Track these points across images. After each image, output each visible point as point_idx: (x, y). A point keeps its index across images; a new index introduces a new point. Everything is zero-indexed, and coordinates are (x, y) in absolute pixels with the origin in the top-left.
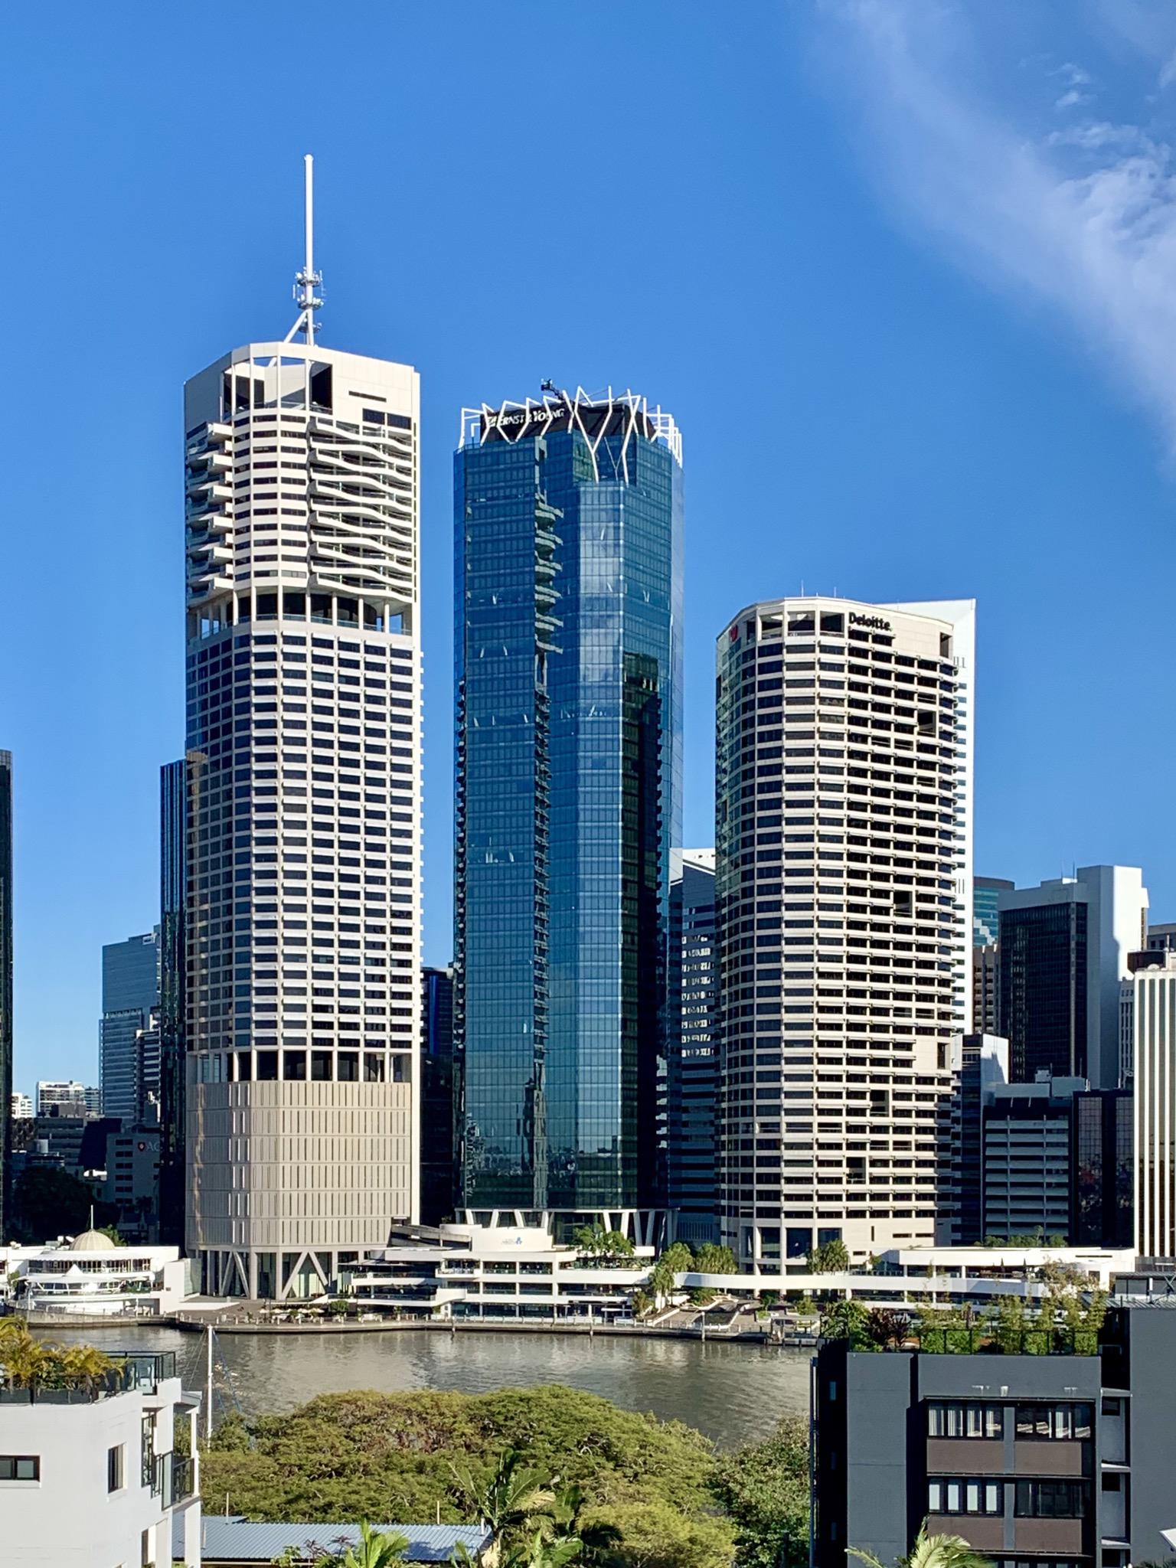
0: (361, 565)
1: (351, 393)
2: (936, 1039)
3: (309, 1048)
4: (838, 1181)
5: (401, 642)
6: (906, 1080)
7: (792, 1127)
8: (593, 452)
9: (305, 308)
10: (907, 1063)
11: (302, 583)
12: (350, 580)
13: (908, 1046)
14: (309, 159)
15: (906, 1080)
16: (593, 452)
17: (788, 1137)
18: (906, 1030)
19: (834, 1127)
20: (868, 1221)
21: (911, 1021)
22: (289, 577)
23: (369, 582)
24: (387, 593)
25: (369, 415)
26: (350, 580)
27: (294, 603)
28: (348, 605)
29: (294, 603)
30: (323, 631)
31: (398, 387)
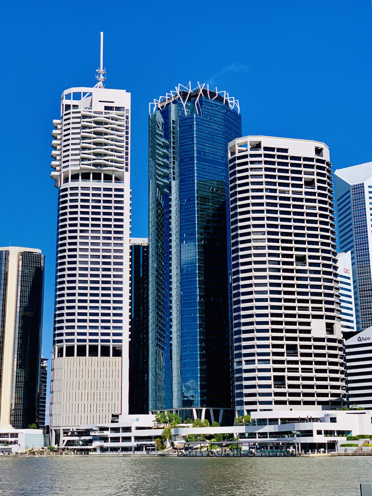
1: (100, 101)
2: (325, 321)
4: (269, 386)
5: (118, 186)
6: (309, 339)
7: (247, 362)
8: (184, 105)
9: (99, 81)
10: (309, 332)
13: (308, 324)
14: (102, 33)
15: (309, 339)
16: (184, 105)
17: (245, 367)
18: (307, 316)
21: (310, 312)
22: (74, 167)
23: (106, 166)
25: (106, 108)
27: (75, 177)
31: (122, 98)
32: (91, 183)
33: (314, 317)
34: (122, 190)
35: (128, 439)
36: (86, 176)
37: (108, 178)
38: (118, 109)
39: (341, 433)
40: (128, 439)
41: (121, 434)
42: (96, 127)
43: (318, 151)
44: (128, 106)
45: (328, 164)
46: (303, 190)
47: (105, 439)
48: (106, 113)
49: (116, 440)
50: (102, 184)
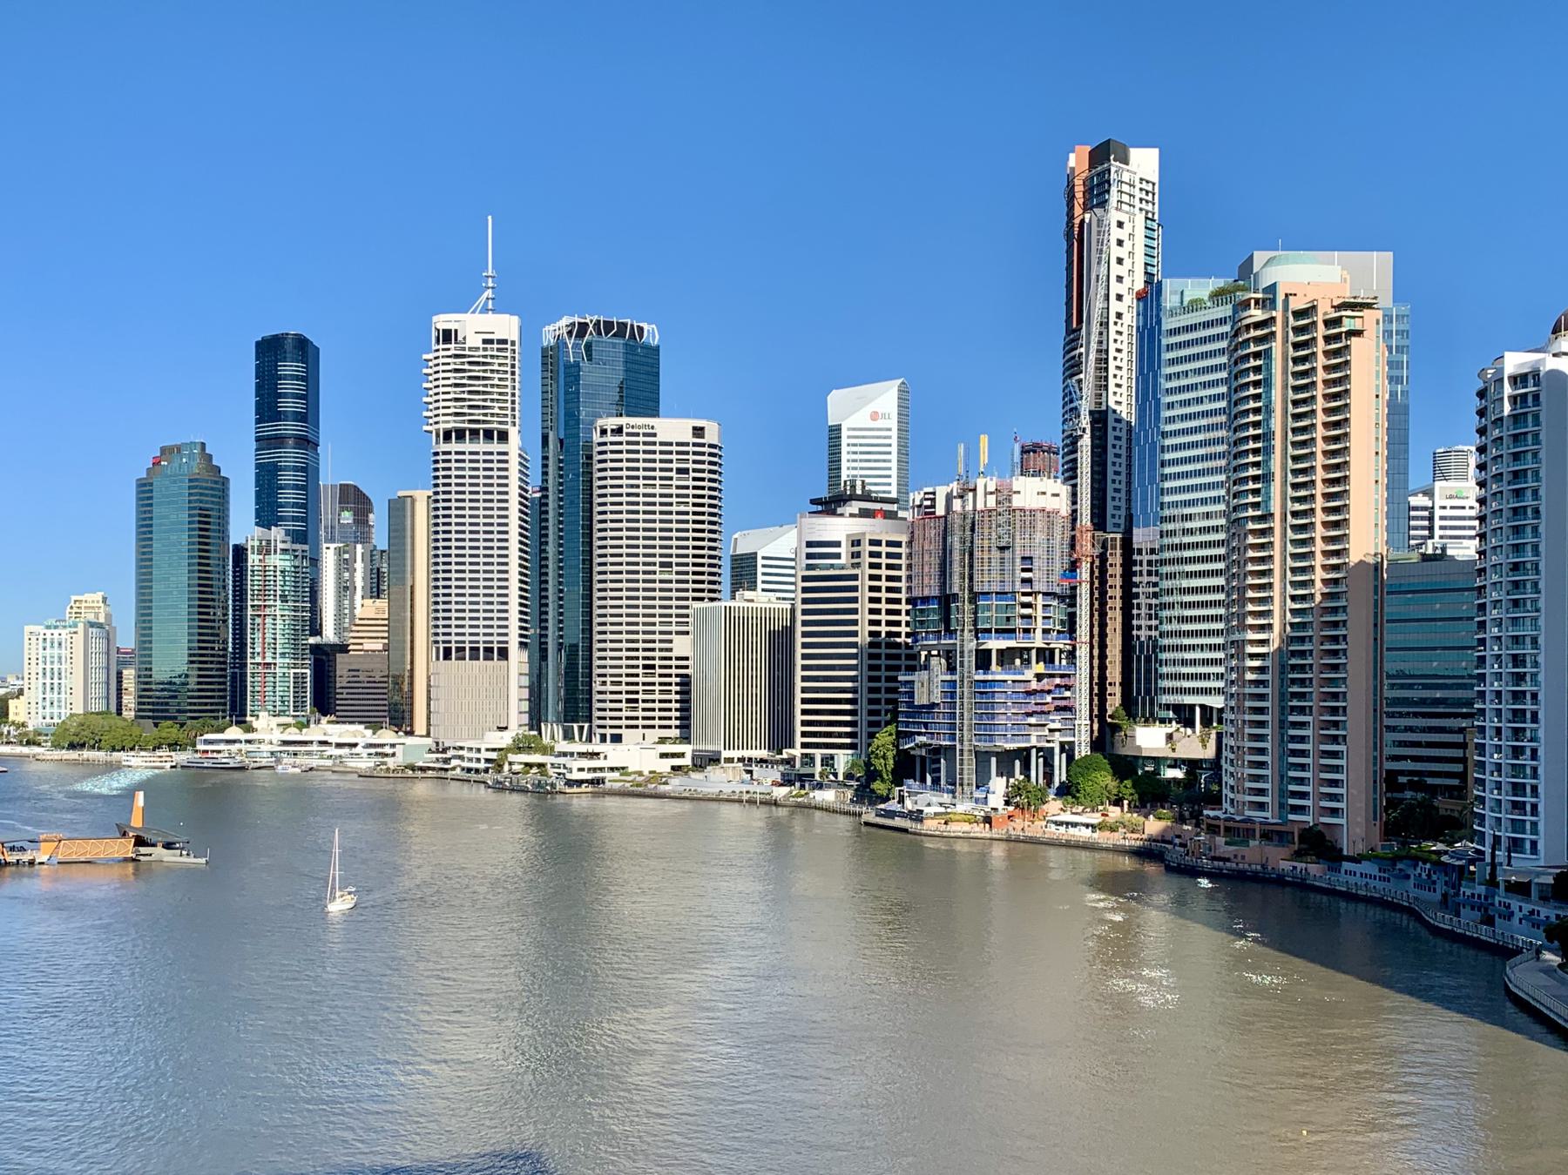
0: (478, 414)
3: (453, 646)
10: (670, 650)
11: (449, 426)
12: (470, 421)
13: (671, 641)
19: (620, 683)
20: (641, 731)
21: (674, 628)
23: (484, 422)
24: (495, 426)
25: (485, 341)
26: (470, 421)
27: (447, 436)
28: (475, 433)
29: (447, 436)
31: (507, 326)
32: (467, 446)
33: (678, 633)
34: (506, 454)
35: (478, 760)
36: (460, 435)
37: (489, 435)
39: (612, 769)
40: (478, 760)
41: (474, 755)
42: (473, 369)
43: (698, 431)
44: (515, 336)
45: (711, 446)
46: (674, 483)
47: (461, 758)
48: (485, 349)
49: (470, 760)
50: (482, 446)
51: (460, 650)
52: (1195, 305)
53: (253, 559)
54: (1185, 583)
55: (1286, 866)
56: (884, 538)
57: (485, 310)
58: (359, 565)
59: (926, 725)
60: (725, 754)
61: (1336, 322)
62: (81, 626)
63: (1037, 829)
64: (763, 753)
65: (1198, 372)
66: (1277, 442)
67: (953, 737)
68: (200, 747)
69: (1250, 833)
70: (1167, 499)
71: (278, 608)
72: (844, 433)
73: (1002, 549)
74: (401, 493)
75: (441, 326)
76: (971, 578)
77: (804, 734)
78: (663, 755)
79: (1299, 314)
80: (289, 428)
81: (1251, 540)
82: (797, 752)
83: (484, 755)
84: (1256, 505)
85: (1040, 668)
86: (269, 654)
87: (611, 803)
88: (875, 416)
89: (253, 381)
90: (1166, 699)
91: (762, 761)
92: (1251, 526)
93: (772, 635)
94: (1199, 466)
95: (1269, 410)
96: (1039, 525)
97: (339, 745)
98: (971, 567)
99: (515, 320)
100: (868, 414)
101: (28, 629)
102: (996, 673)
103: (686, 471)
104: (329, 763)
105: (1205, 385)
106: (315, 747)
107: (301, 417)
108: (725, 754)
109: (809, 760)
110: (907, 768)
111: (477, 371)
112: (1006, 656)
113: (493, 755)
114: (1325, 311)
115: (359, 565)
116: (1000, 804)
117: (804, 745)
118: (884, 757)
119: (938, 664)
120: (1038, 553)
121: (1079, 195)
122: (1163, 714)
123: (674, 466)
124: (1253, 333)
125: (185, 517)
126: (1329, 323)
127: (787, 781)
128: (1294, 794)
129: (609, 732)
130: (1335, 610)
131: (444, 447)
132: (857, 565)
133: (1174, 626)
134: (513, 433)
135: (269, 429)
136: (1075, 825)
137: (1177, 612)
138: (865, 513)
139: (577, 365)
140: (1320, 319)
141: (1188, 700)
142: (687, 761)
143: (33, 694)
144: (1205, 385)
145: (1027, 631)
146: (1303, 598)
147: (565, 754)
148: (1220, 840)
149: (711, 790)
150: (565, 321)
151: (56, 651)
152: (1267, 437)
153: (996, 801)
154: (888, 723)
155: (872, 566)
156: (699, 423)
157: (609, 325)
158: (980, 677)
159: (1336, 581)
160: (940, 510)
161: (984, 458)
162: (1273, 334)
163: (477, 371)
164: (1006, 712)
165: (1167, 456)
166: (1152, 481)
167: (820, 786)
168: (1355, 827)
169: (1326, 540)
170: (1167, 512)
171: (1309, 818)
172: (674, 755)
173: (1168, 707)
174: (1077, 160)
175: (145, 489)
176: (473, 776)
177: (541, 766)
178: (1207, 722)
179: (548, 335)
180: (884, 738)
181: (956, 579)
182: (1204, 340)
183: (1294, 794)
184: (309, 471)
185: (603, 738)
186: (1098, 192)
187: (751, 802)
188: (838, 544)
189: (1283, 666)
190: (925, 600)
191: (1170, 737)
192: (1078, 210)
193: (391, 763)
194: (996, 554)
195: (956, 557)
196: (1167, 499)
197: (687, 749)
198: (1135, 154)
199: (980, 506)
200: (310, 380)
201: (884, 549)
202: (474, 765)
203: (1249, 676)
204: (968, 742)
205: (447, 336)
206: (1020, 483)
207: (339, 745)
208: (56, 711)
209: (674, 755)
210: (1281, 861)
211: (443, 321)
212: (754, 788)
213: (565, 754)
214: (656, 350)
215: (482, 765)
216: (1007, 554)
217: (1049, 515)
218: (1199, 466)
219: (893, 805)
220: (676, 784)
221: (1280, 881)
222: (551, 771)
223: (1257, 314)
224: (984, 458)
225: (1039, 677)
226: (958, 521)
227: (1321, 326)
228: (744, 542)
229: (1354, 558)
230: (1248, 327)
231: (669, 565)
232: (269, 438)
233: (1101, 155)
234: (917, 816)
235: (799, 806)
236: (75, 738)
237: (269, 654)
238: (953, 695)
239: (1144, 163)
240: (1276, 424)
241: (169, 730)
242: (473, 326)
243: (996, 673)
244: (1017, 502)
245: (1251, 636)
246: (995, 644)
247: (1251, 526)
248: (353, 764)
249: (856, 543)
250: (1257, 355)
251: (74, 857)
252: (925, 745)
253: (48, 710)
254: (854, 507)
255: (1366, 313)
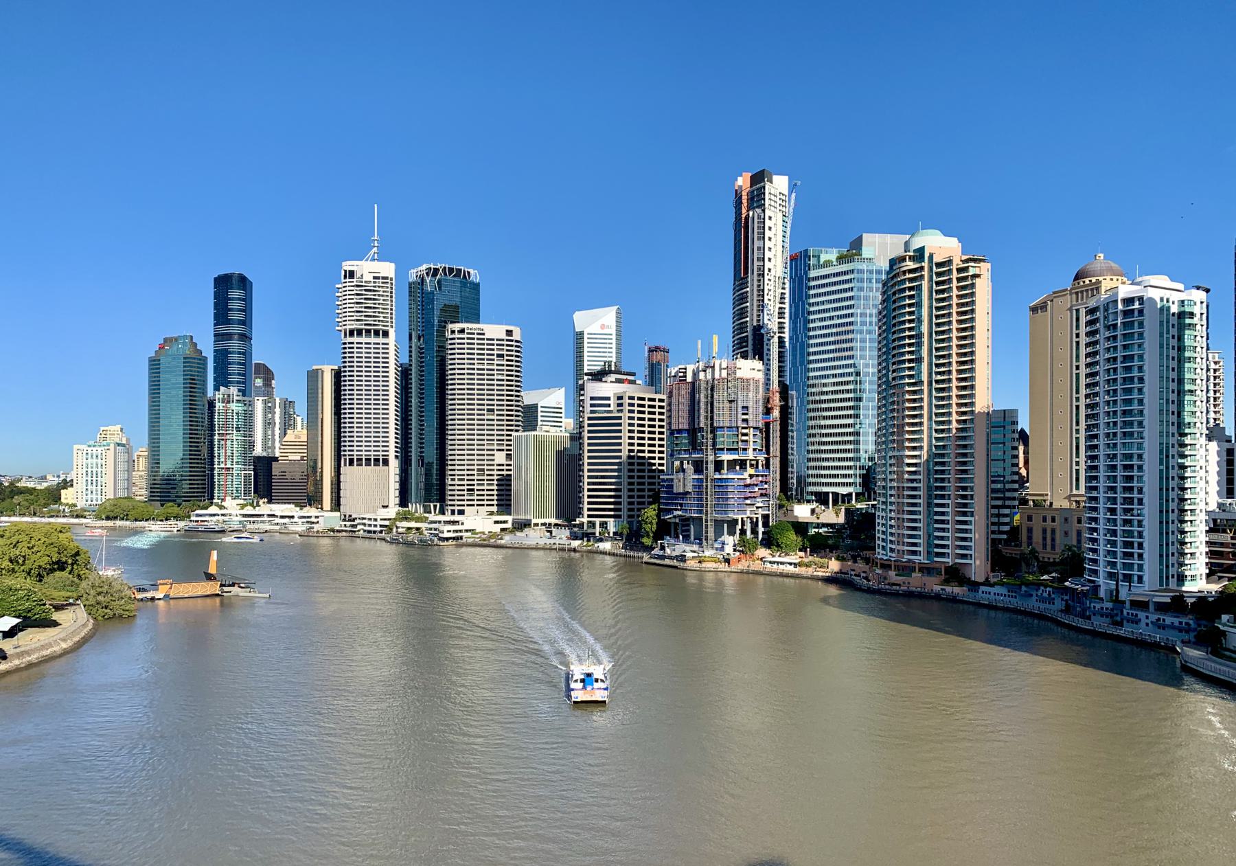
5: (385, 340)
21: (496, 447)
27: (352, 333)
28: (368, 331)
29: (352, 333)
30: (368, 340)
31: (387, 269)
32: (364, 339)
36: (360, 332)
37: (377, 333)
38: (384, 278)
41: (373, 523)
42: (368, 293)
43: (509, 333)
44: (392, 274)
50: (373, 339)
51: (377, 460)
52: (828, 264)
53: (219, 406)
54: (823, 422)
55: (937, 588)
56: (636, 395)
57: (373, 260)
58: (277, 410)
59: (681, 505)
60: (534, 521)
61: (965, 269)
62: (112, 446)
63: (757, 566)
64: (553, 521)
65: (830, 302)
66: (925, 339)
67: (700, 512)
68: (193, 518)
69: (913, 570)
70: (811, 374)
71: (235, 435)
72: (586, 336)
73: (730, 402)
74: (315, 367)
75: (348, 268)
76: (712, 418)
77: (589, 510)
78: (496, 522)
79: (939, 265)
80: (235, 329)
81: (907, 397)
82: (585, 520)
83: (379, 522)
84: (911, 377)
85: (752, 471)
86: (229, 463)
87: (464, 549)
88: (603, 327)
89: (212, 301)
90: (810, 489)
91: (556, 525)
92: (907, 388)
93: (560, 454)
94: (831, 356)
95: (920, 321)
96: (752, 387)
97: (282, 517)
98: (712, 411)
99: (392, 266)
100: (598, 325)
101: (76, 447)
102: (725, 474)
103: (502, 356)
104: (277, 528)
105: (835, 309)
106: (266, 518)
107: (243, 323)
108: (534, 521)
109: (592, 524)
110: (664, 529)
111: (370, 295)
112: (732, 464)
113: (387, 523)
114: (957, 263)
115: (277, 410)
116: (731, 551)
117: (589, 516)
118: (651, 523)
119: (690, 468)
120: (750, 404)
121: (745, 201)
122: (809, 497)
123: (495, 352)
124: (908, 276)
125: (181, 380)
126: (959, 270)
127: (574, 537)
128: (938, 546)
129: (457, 508)
130: (964, 438)
131: (349, 339)
132: (621, 411)
133: (816, 447)
134: (392, 332)
135: (223, 329)
136: (782, 563)
137: (818, 439)
138: (618, 381)
139: (432, 293)
140: (954, 267)
141: (825, 489)
142: (509, 525)
143: (80, 485)
144: (835, 309)
145: (745, 449)
146: (942, 431)
147: (435, 522)
148: (892, 573)
149: (528, 542)
150: (424, 267)
151: (95, 460)
152: (919, 336)
153: (729, 549)
154: (650, 503)
155: (630, 411)
156: (510, 328)
157: (451, 270)
158: (717, 476)
159: (965, 421)
160: (689, 379)
161: (715, 348)
162: (922, 276)
163: (370, 295)
164: (734, 497)
165: (811, 350)
166: (802, 363)
167: (601, 540)
168: (978, 566)
169: (959, 397)
170: (811, 382)
171: (949, 560)
172: (501, 522)
173: (812, 493)
174: (743, 181)
175: (155, 364)
176: (372, 535)
177: (418, 529)
178: (835, 503)
179: (413, 275)
180: (650, 513)
181: (702, 419)
182: (834, 284)
183: (938, 546)
184: (247, 354)
185: (453, 512)
186: (757, 199)
187: (551, 549)
188: (609, 399)
189: (929, 470)
190: (680, 431)
191: (813, 511)
192: (744, 211)
193: (316, 527)
194: (727, 405)
195: (702, 406)
196: (811, 374)
197: (509, 518)
198: (775, 178)
199: (717, 376)
200: (247, 300)
201: (636, 402)
202: (372, 529)
203: (906, 476)
204: (711, 515)
205: (352, 274)
206: (741, 363)
207: (282, 517)
208: (94, 497)
209: (501, 522)
210: (934, 585)
211: (348, 266)
212: (552, 541)
213: (435, 522)
214: (476, 287)
215: (378, 529)
216: (733, 405)
217: (757, 381)
218: (831, 356)
219: (656, 551)
220: (507, 539)
221: (937, 597)
222: (426, 532)
223: (911, 265)
224: (715, 348)
225: (751, 476)
226: (703, 386)
227: (955, 272)
228: (528, 398)
229: (978, 408)
230: (904, 273)
231: (493, 410)
232: (223, 335)
233: (759, 179)
234: (682, 558)
235: (590, 552)
236: (112, 512)
237: (229, 463)
238: (700, 487)
239: (779, 185)
240: (925, 329)
241: (172, 508)
242: (367, 269)
243: (725, 474)
244: (739, 374)
245: (908, 453)
246: (726, 457)
247: (907, 388)
248: (293, 528)
249: (620, 398)
250: (910, 289)
251: (181, 595)
252: (679, 516)
253: (89, 496)
254: (613, 377)
255: (982, 264)
